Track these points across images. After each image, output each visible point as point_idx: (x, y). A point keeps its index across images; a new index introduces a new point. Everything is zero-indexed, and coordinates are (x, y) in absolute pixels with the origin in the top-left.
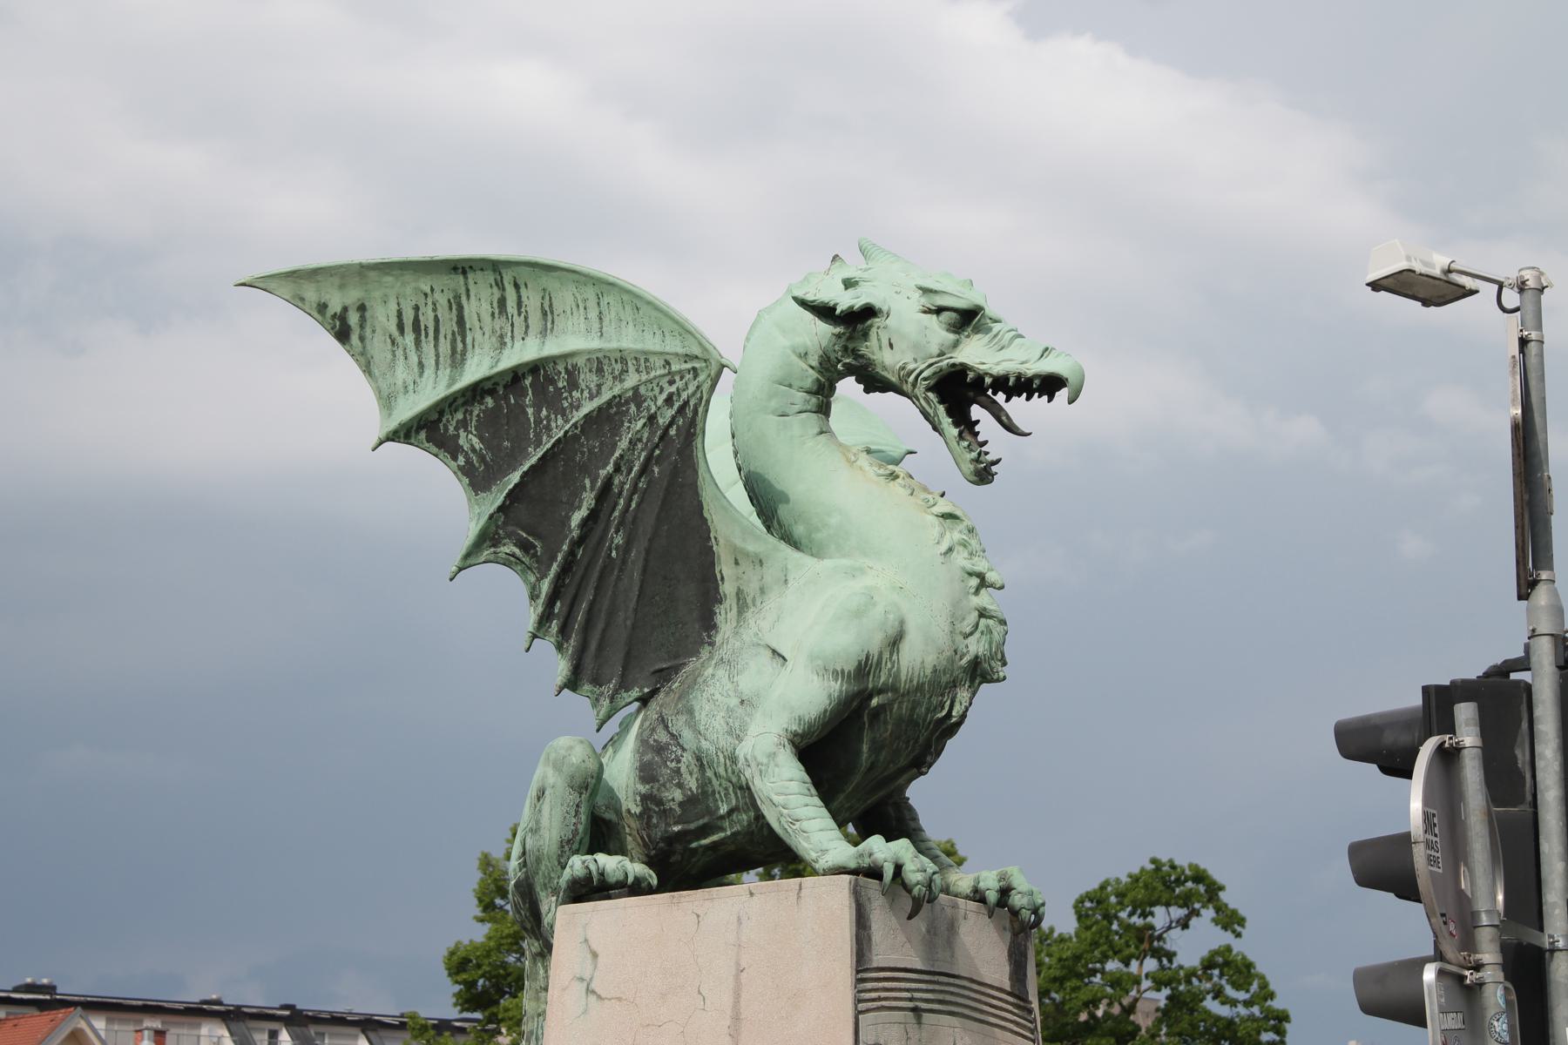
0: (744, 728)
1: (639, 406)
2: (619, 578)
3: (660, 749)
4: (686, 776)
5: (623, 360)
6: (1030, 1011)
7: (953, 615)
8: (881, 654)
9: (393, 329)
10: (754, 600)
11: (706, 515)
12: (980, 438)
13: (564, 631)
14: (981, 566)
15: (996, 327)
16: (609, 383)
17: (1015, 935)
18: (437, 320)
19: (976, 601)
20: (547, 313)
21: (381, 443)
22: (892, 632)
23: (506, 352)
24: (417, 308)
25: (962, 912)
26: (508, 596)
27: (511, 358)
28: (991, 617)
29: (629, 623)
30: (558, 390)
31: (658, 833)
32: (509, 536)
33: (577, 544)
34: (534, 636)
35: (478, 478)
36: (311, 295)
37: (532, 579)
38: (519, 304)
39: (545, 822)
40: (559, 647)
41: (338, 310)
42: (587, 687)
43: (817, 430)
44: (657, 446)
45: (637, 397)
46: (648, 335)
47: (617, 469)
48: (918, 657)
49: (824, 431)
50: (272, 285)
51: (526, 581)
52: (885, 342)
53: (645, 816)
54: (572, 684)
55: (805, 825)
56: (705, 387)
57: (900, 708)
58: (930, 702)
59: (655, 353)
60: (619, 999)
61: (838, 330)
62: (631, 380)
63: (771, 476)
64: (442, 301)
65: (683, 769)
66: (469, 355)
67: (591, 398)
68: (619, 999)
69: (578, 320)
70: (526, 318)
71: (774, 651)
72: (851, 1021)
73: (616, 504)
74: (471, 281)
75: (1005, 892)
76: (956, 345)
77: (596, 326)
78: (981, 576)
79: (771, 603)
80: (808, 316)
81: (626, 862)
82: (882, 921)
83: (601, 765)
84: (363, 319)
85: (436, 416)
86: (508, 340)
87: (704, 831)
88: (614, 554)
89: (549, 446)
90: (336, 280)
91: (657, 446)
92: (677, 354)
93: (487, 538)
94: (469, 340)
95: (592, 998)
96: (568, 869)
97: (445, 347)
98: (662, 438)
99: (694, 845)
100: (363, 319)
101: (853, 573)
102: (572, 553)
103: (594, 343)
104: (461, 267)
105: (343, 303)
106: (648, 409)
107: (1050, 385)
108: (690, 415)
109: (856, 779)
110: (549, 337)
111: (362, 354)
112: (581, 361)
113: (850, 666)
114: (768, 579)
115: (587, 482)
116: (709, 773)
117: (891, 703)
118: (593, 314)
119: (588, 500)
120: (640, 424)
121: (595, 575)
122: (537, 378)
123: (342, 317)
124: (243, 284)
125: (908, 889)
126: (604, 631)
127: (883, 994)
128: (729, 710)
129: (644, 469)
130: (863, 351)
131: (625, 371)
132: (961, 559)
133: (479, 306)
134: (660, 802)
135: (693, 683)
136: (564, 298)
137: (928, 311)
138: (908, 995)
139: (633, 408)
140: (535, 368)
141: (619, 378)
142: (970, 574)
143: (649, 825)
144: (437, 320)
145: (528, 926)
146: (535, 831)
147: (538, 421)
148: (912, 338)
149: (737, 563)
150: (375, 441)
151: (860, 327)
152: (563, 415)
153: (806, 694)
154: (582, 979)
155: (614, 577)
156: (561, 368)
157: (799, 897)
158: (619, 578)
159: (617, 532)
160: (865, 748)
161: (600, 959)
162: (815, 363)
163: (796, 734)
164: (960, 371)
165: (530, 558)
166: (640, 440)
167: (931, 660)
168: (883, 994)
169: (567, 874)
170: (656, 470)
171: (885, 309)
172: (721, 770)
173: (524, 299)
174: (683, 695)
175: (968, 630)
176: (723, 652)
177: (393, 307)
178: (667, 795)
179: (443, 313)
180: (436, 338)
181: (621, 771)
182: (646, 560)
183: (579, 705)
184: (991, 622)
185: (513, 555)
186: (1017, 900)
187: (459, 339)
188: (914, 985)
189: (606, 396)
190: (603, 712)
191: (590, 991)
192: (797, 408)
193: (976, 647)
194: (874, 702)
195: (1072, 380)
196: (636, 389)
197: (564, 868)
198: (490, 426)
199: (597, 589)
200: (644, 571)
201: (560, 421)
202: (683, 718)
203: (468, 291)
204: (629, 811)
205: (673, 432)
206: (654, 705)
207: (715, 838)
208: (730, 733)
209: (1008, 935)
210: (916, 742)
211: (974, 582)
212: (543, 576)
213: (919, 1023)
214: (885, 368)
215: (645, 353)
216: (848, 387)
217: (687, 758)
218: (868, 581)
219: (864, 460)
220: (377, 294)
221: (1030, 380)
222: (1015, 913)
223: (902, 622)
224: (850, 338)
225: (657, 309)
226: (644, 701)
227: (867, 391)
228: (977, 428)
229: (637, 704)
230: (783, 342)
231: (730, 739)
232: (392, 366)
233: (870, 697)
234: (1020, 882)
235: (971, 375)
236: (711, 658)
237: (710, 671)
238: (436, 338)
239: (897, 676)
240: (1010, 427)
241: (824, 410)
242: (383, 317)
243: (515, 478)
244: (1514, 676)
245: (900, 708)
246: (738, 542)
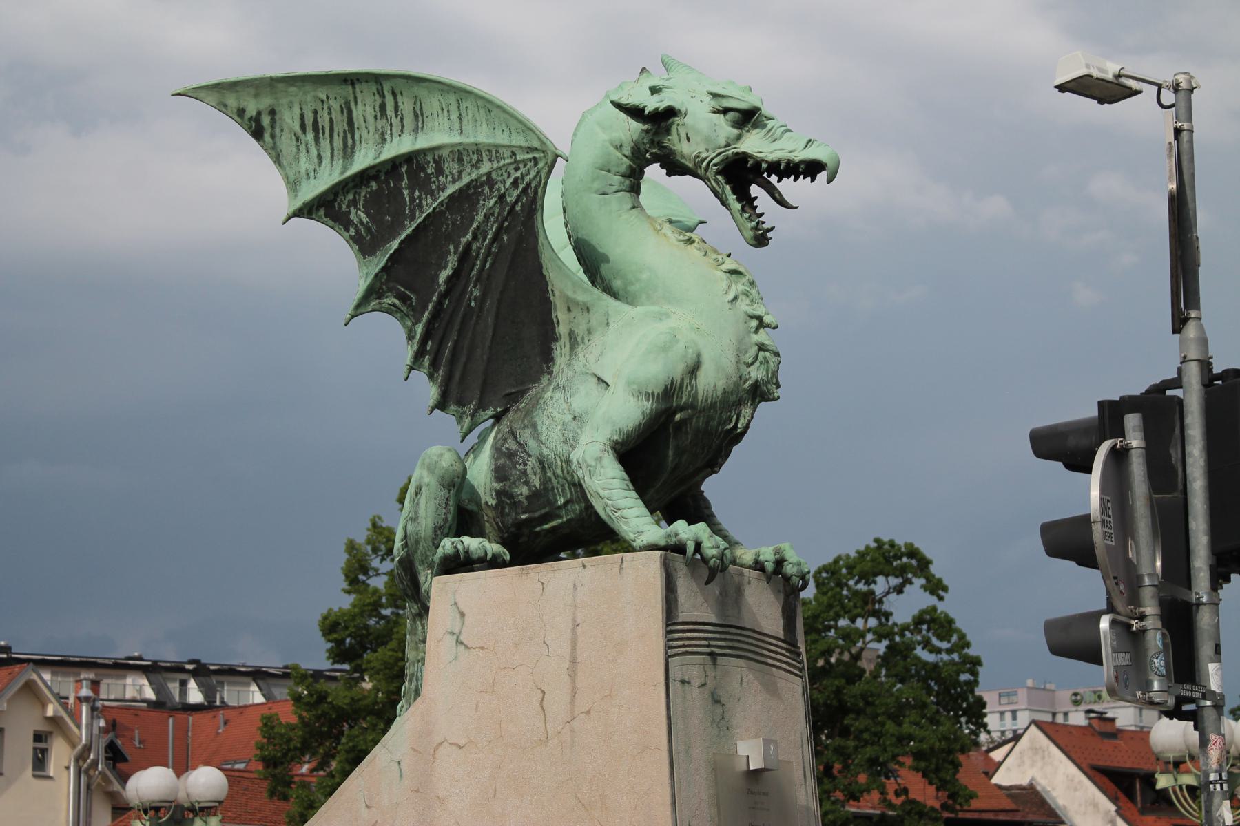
0: (576, 438)
1: (491, 188)
2: (477, 323)
3: (511, 455)
4: (531, 476)
5: (479, 152)
6: (799, 654)
7: (738, 349)
8: (682, 380)
9: (297, 127)
10: (583, 338)
11: (545, 272)
12: (758, 211)
13: (434, 365)
14: (759, 311)
15: (770, 124)
16: (468, 170)
17: (787, 596)
18: (331, 121)
19: (756, 338)
20: (418, 115)
21: (289, 218)
22: (691, 362)
23: (387, 146)
24: (315, 112)
25: (746, 579)
26: (390, 336)
27: (391, 151)
28: (768, 351)
29: (485, 357)
30: (428, 177)
31: (510, 520)
32: (390, 290)
33: (443, 296)
34: (411, 368)
35: (365, 246)
36: (232, 102)
37: (409, 324)
38: (396, 108)
39: (422, 512)
40: (431, 377)
41: (254, 114)
42: (453, 407)
43: (630, 205)
44: (506, 219)
45: (490, 181)
46: (498, 132)
47: (475, 237)
48: (710, 382)
49: (636, 206)
50: (202, 94)
51: (404, 325)
52: (683, 136)
53: (499, 507)
54: (442, 405)
55: (625, 513)
56: (543, 173)
57: (697, 421)
59: (503, 146)
60: (482, 648)
61: (646, 127)
62: (485, 168)
63: (594, 242)
64: (335, 105)
65: (529, 470)
66: (357, 148)
67: (454, 182)
68: (482, 648)
69: (443, 120)
70: (402, 120)
71: (599, 379)
72: (663, 662)
73: (474, 264)
74: (358, 91)
75: (779, 563)
76: (739, 138)
77: (457, 125)
78: (760, 318)
79: (596, 341)
80: (623, 115)
81: (486, 543)
82: (685, 585)
83: (465, 469)
84: (273, 122)
86: (388, 137)
87: (546, 518)
88: (473, 304)
89: (421, 219)
90: (252, 91)
91: (506, 219)
92: (521, 147)
93: (373, 293)
94: (357, 137)
95: (461, 648)
96: (440, 549)
97: (338, 142)
98: (509, 213)
99: (538, 529)
100: (273, 122)
101: (661, 317)
102: (440, 303)
103: (456, 139)
104: (350, 80)
105: (256, 107)
106: (499, 190)
107: (812, 169)
108: (531, 194)
110: (420, 134)
111: (274, 148)
112: (445, 153)
113: (659, 390)
114: (593, 322)
115: (452, 248)
116: (549, 474)
117: (691, 418)
118: (455, 116)
119: (452, 261)
120: (492, 201)
121: (459, 320)
122: (413, 166)
123: (257, 119)
124: (179, 94)
125: (704, 560)
126: (466, 364)
127: (687, 642)
128: (564, 424)
129: (496, 237)
130: (666, 143)
131: (480, 160)
132: (744, 306)
133: (364, 110)
134: (511, 496)
135: (535, 404)
136: (432, 103)
137: (717, 112)
139: (487, 190)
140: (409, 158)
141: (476, 166)
142: (752, 317)
143: (502, 514)
144: (331, 121)
145: (409, 593)
146: (414, 519)
147: (412, 200)
148: (703, 133)
149: (569, 310)
150: (284, 217)
151: (663, 124)
152: (432, 195)
153: (624, 411)
154: (452, 633)
155: (472, 322)
156: (430, 158)
157: (621, 568)
158: (477, 323)
159: (475, 286)
160: (671, 453)
161: (468, 619)
162: (627, 153)
163: (617, 442)
164: (743, 158)
165: (407, 309)
166: (493, 214)
167: (721, 384)
168: (687, 642)
169: (440, 552)
170: (505, 238)
171: (683, 110)
172: (559, 471)
173: (400, 104)
174: (528, 413)
175: (750, 360)
176: (560, 379)
177: (297, 111)
178: (516, 491)
179: (336, 115)
180: (331, 136)
181: (480, 472)
182: (498, 308)
183: (447, 421)
184: (767, 354)
185: (394, 305)
186: (789, 569)
187: (349, 136)
188: (710, 635)
189: (466, 180)
190: (466, 427)
191: (459, 642)
192: (614, 188)
193: (756, 373)
194: (678, 417)
195: (830, 164)
196: (489, 174)
197: (437, 547)
198: (374, 205)
199: (460, 331)
200: (497, 316)
201: (430, 200)
202: (528, 431)
203: (355, 98)
204: (486, 503)
205: (518, 208)
206: (505, 421)
207: (554, 523)
208: (565, 442)
209: (782, 596)
211: (755, 323)
212: (418, 321)
213: (715, 663)
214: (683, 156)
215: (495, 146)
216: (654, 172)
217: (532, 462)
218: (672, 323)
219: (667, 229)
220: (284, 101)
221: (797, 165)
222: (787, 579)
223: (699, 355)
224: (656, 134)
225: (505, 111)
226: (498, 418)
227: (669, 174)
228: (755, 203)
229: (491, 421)
230: (603, 137)
231: (565, 447)
232: (297, 158)
233: (675, 413)
234: (791, 555)
235: (751, 161)
236: (549, 384)
237: (549, 394)
238: (331, 136)
240: (782, 202)
241: (635, 189)
242: (290, 119)
243: (395, 244)
244: (1169, 393)
245: (697, 421)
246: (570, 294)
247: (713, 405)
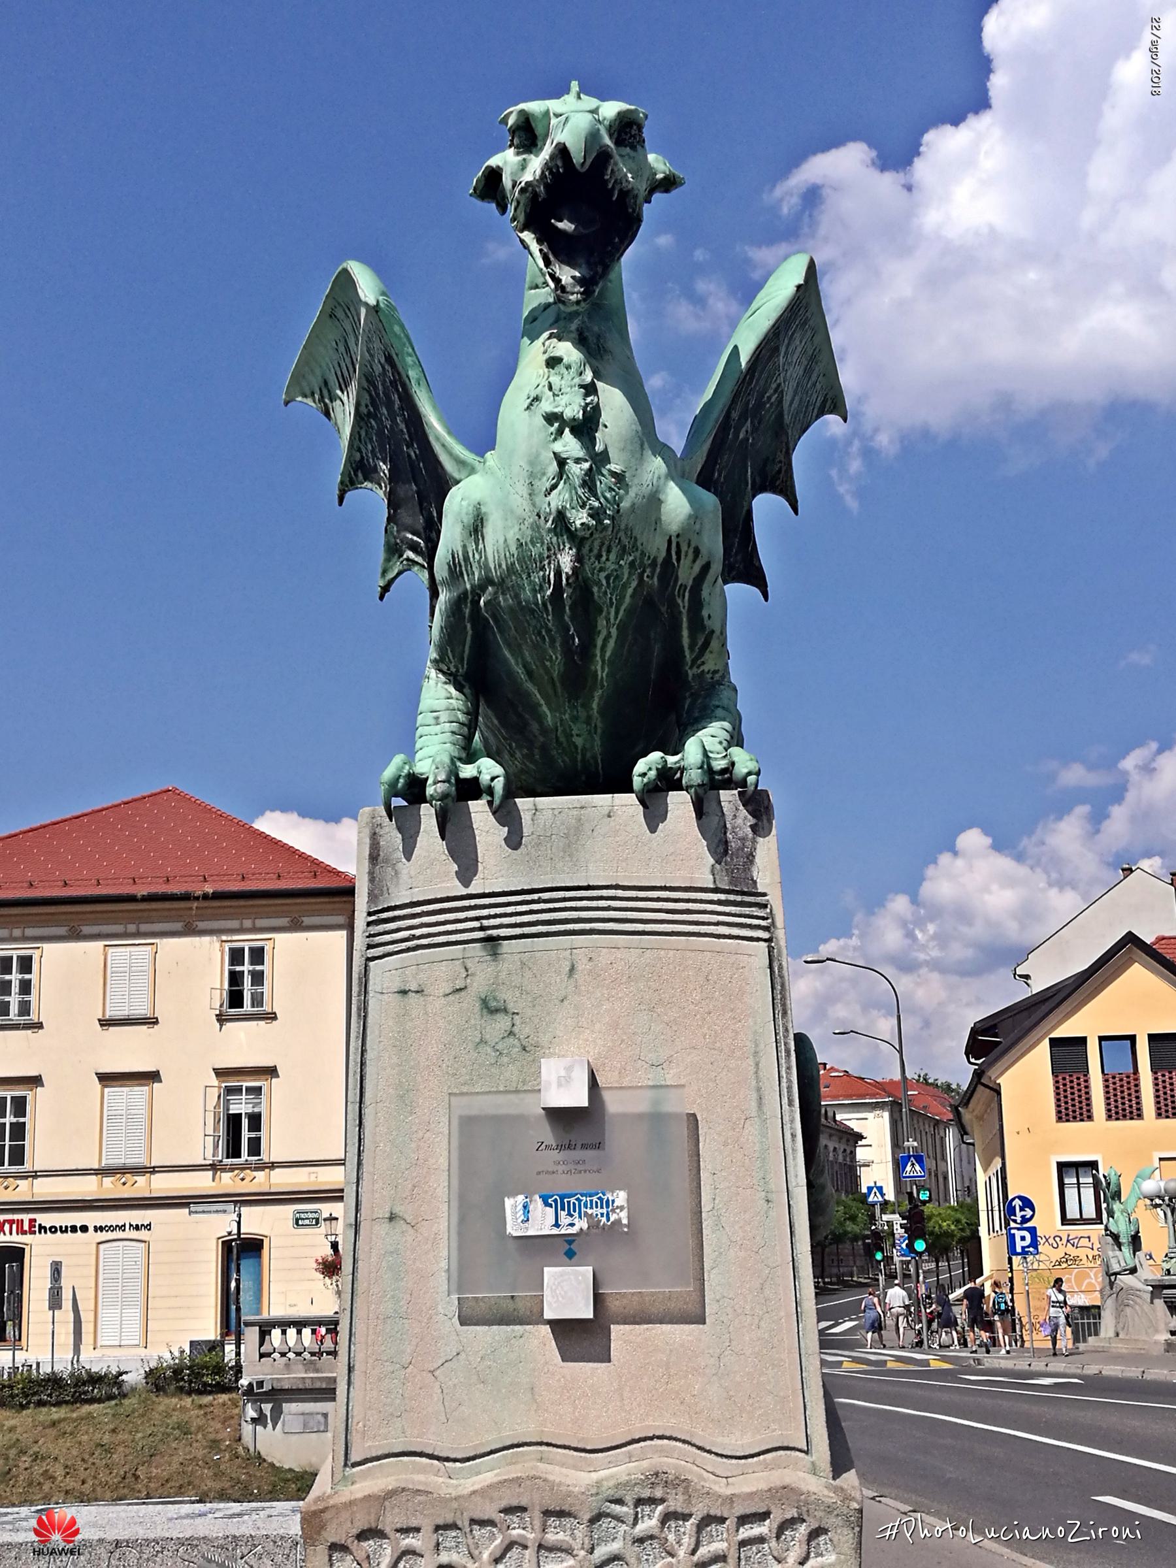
8: (464, 547)
22: (468, 520)
58: (531, 582)
85: (358, 456)
109: (530, 686)
132: (547, 406)
138: (476, 924)
167: (513, 535)
168: (417, 932)
175: (548, 485)
188: (485, 912)
210: (549, 631)
213: (495, 954)
247: (511, 569)
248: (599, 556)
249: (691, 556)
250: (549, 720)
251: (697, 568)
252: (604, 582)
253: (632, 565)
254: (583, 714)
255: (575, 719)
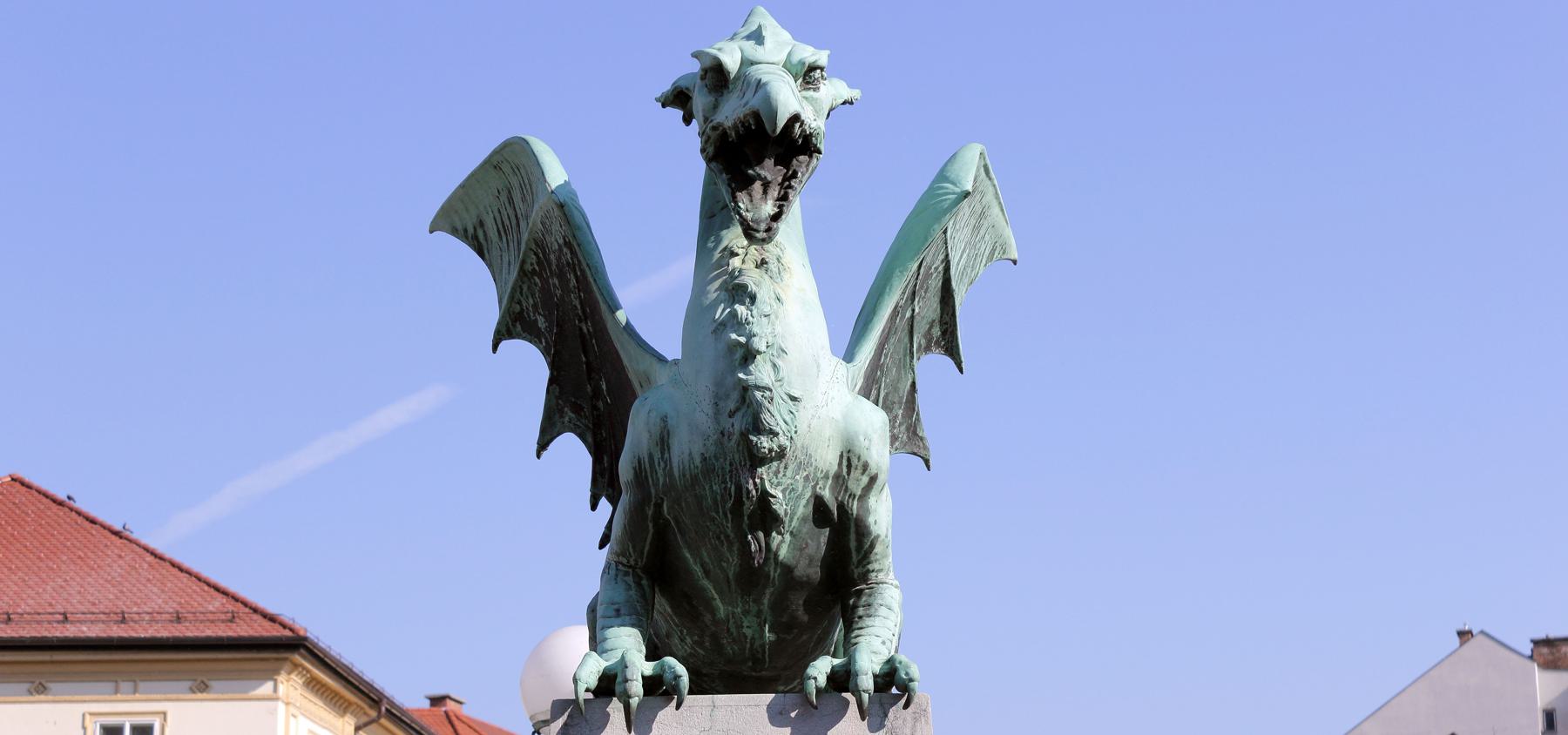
8: (651, 456)
37: (590, 440)
64: (504, 198)
167: (697, 449)
210: (727, 537)
211: (739, 354)
223: (664, 419)
239: (669, 474)
247: (695, 478)
248: (777, 473)
249: (859, 471)
250: (722, 609)
251: (865, 479)
252: (780, 495)
253: (807, 478)
254: (754, 609)
255: (746, 612)
